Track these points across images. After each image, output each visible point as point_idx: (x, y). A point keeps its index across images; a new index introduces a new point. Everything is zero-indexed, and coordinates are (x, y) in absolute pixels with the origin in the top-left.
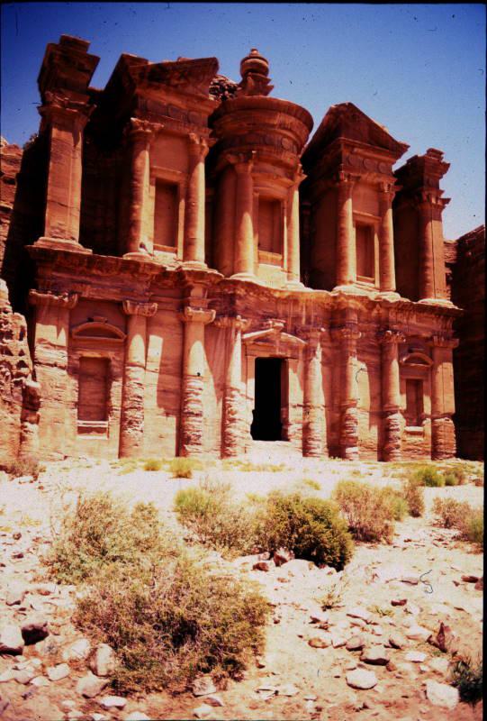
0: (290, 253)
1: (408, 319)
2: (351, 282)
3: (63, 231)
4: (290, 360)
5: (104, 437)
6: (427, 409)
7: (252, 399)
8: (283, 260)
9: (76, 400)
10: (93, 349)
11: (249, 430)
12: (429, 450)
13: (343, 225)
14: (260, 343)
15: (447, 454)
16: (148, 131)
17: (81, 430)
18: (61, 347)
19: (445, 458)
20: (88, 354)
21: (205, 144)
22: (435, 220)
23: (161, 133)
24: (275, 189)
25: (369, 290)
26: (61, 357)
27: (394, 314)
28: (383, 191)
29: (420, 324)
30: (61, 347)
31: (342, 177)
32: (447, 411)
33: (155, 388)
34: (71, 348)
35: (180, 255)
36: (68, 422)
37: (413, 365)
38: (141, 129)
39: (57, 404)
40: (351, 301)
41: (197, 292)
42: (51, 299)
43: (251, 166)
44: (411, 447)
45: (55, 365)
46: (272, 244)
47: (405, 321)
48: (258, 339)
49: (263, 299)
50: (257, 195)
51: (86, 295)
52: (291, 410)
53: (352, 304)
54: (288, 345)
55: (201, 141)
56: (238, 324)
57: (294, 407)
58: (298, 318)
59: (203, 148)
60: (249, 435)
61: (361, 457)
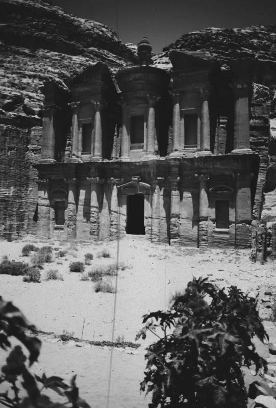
0: (147, 141)
1: (213, 165)
2: (176, 150)
3: (46, 156)
4: (145, 195)
5: (62, 231)
6: (232, 218)
7: (125, 215)
8: (143, 146)
9: (54, 217)
10: (58, 198)
11: (124, 229)
12: (234, 243)
13: (173, 120)
14: (127, 189)
15: (242, 246)
16: (75, 106)
17: (56, 229)
18: (46, 199)
19: (241, 248)
20: (57, 200)
21: (98, 103)
22: (241, 97)
23: (80, 105)
24: (137, 111)
25: (193, 153)
26: (47, 202)
27: (203, 164)
28: (200, 92)
29: (224, 167)
30: (46, 199)
31: (171, 94)
32: (242, 220)
33: (82, 212)
34: (50, 198)
35: (92, 155)
36: (51, 226)
37: (220, 192)
38: (73, 106)
39: (44, 219)
40: (172, 161)
41: (93, 170)
42: (41, 182)
43: (125, 104)
44: (219, 241)
45: (43, 205)
46: (137, 139)
47: (211, 167)
48: (126, 187)
49: (132, 167)
50: (129, 117)
51: (53, 178)
52: (145, 220)
53: (172, 162)
54: (144, 188)
55: (97, 103)
56: (113, 182)
57: (147, 218)
58: (149, 174)
59: (97, 105)
60: (125, 232)
61: (181, 244)
